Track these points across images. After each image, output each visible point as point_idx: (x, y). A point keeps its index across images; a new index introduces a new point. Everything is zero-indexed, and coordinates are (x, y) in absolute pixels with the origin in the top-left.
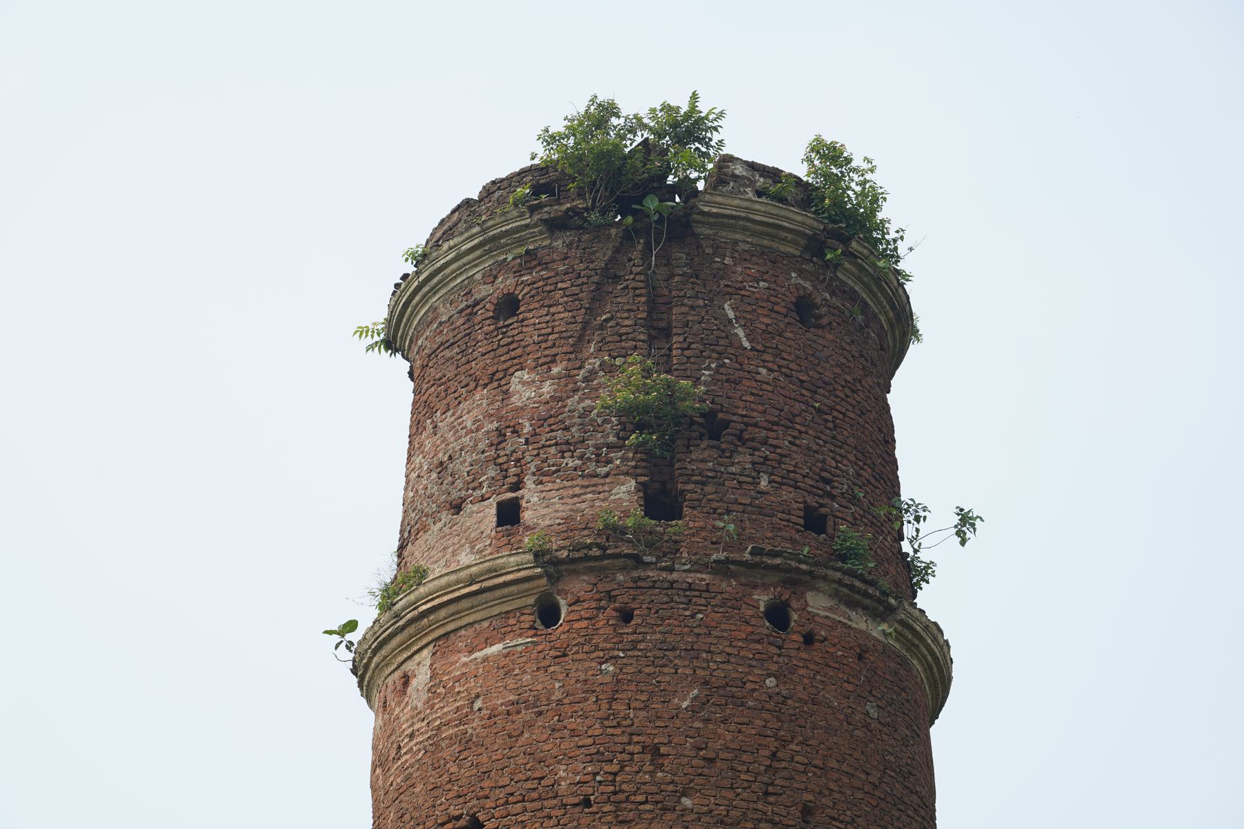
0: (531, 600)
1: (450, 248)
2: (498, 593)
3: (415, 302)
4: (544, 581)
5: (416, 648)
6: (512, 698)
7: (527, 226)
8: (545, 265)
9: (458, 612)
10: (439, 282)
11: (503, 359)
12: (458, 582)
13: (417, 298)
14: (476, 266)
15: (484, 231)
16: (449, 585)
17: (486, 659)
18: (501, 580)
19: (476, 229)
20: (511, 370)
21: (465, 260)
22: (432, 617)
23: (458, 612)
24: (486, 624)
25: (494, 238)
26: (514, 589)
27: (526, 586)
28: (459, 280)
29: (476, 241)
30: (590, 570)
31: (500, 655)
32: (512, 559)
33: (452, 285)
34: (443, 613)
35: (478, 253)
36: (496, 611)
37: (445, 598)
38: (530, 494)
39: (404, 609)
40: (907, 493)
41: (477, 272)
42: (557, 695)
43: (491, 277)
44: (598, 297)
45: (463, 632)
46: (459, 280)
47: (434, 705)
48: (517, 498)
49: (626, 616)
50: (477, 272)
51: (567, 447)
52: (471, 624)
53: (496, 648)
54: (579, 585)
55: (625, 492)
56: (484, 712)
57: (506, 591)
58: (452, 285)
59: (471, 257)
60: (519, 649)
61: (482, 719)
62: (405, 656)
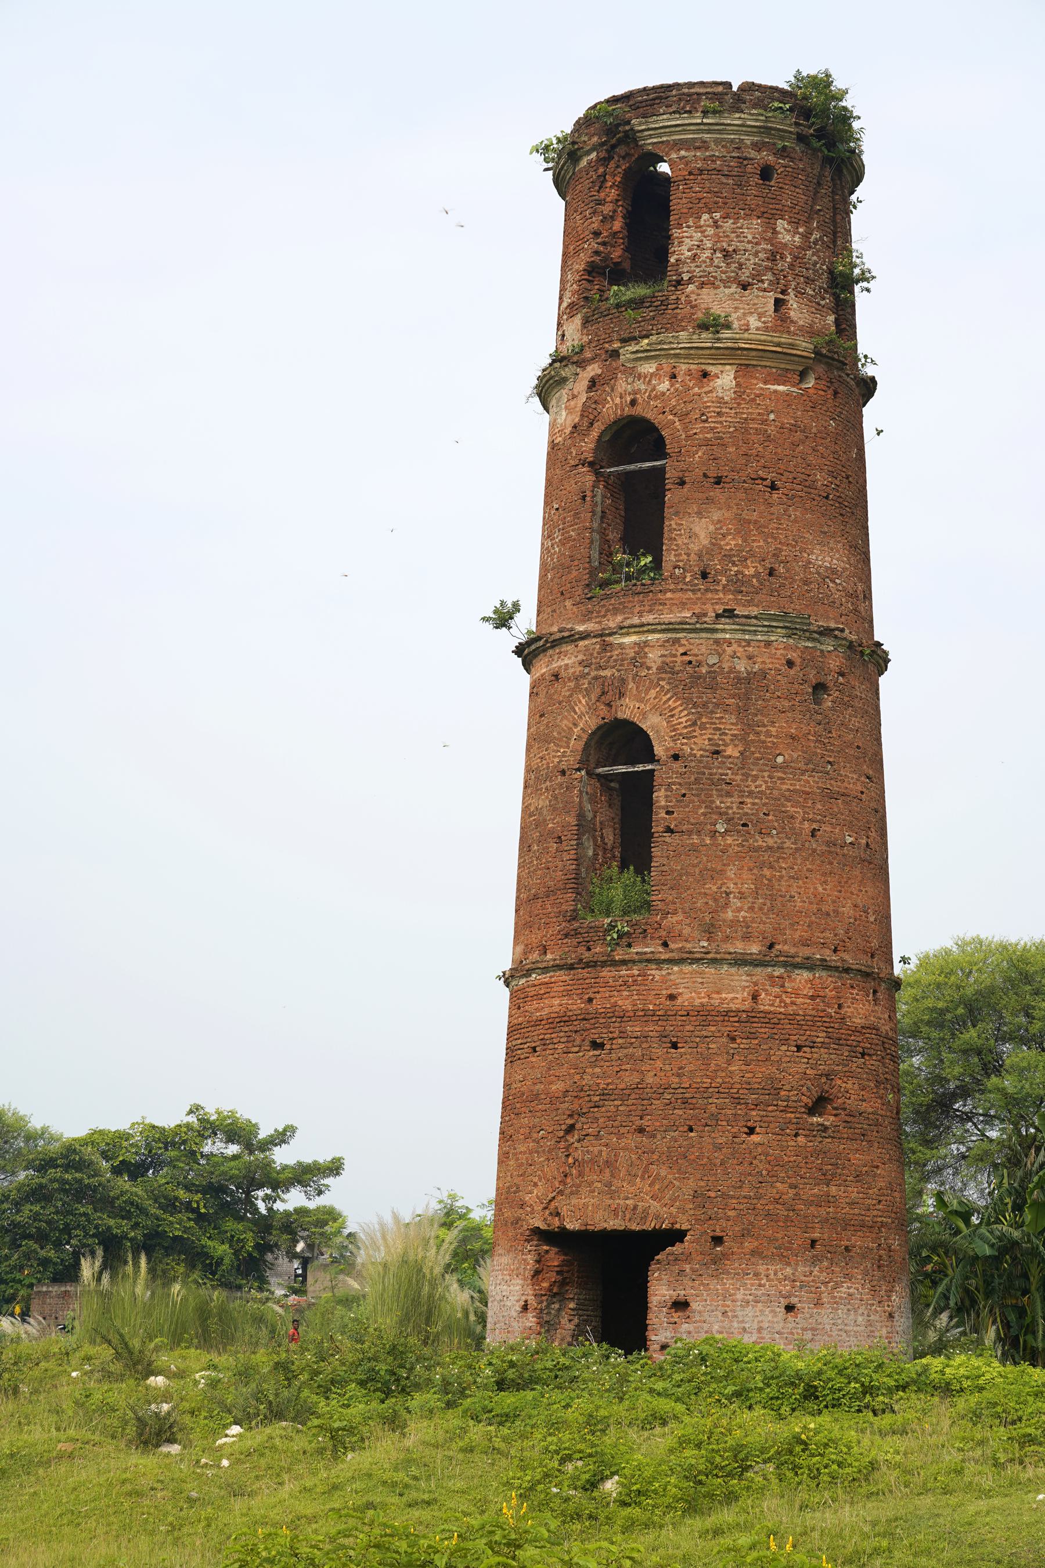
0: (801, 369)
1: (740, 118)
2: (788, 358)
3: (688, 128)
4: (811, 361)
5: (722, 362)
6: (792, 422)
7: (790, 132)
8: (792, 159)
9: (762, 357)
10: (718, 130)
11: (771, 206)
12: (771, 342)
13: (692, 128)
14: (748, 135)
15: (766, 121)
16: (765, 341)
17: (775, 391)
18: (794, 352)
19: (763, 118)
20: (777, 217)
21: (744, 129)
22: (745, 352)
23: (762, 357)
24: (774, 370)
25: (771, 128)
26: (796, 359)
27: (803, 360)
28: (732, 137)
29: (758, 124)
30: (827, 363)
31: (782, 393)
32: (804, 344)
33: (726, 136)
34: (754, 353)
35: (755, 130)
36: (783, 366)
37: (760, 347)
38: (792, 301)
39: (726, 339)
40: (861, 350)
41: (748, 140)
42: (814, 430)
43: (757, 147)
44: (816, 193)
45: (759, 368)
46: (732, 137)
47: (741, 404)
48: (784, 300)
49: (836, 393)
50: (748, 140)
51: (809, 281)
52: (766, 366)
53: (781, 388)
54: (821, 369)
55: (831, 319)
56: (777, 423)
57: (792, 358)
58: (726, 136)
59: (749, 129)
60: (794, 394)
61: (776, 427)
62: (711, 362)
